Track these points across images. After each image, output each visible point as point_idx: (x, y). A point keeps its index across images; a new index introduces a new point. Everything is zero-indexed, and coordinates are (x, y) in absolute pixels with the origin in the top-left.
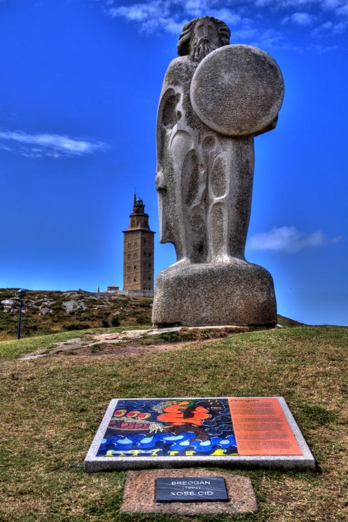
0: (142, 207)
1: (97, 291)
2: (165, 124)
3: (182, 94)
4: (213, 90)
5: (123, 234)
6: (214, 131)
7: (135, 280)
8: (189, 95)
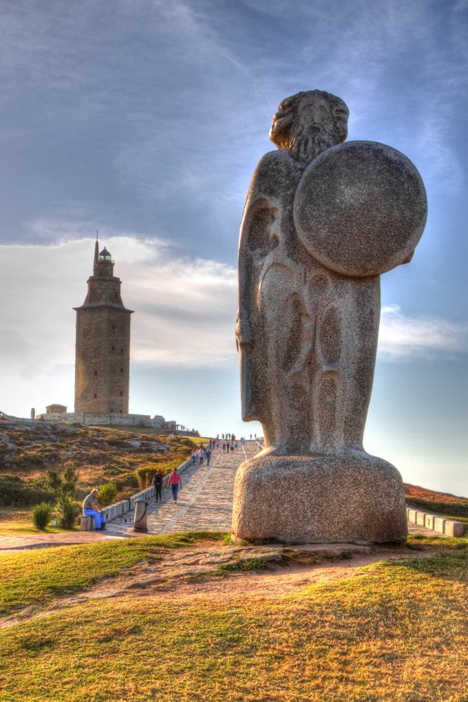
2: (252, 249)
3: (281, 210)
4: (327, 211)
5: (75, 312)
6: (326, 268)
8: (291, 212)
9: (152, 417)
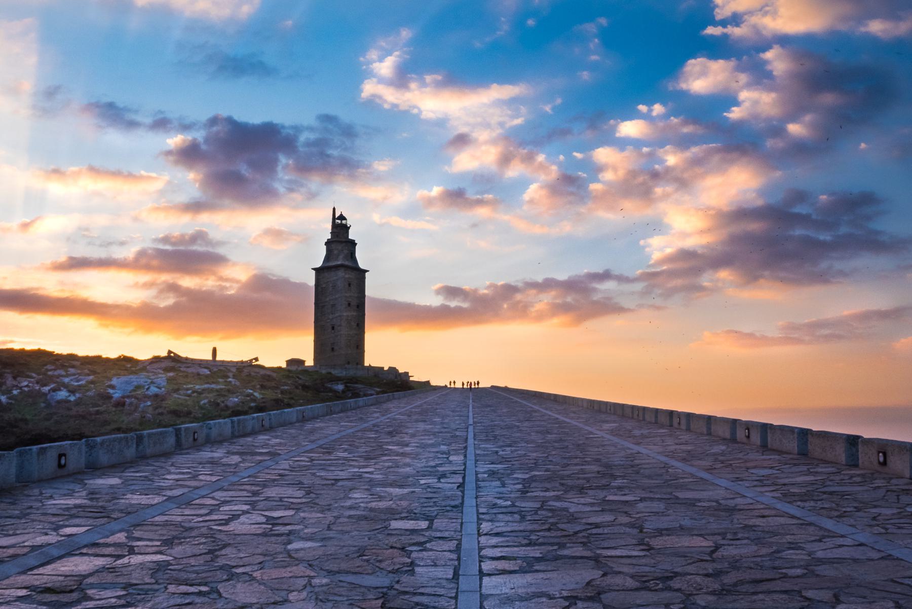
0: (346, 228)
1: (210, 358)
5: (314, 272)
7: (333, 349)
9: (386, 368)
